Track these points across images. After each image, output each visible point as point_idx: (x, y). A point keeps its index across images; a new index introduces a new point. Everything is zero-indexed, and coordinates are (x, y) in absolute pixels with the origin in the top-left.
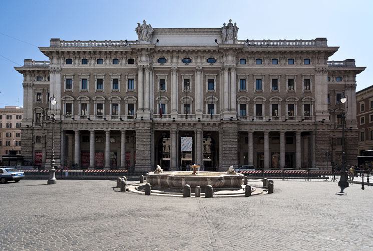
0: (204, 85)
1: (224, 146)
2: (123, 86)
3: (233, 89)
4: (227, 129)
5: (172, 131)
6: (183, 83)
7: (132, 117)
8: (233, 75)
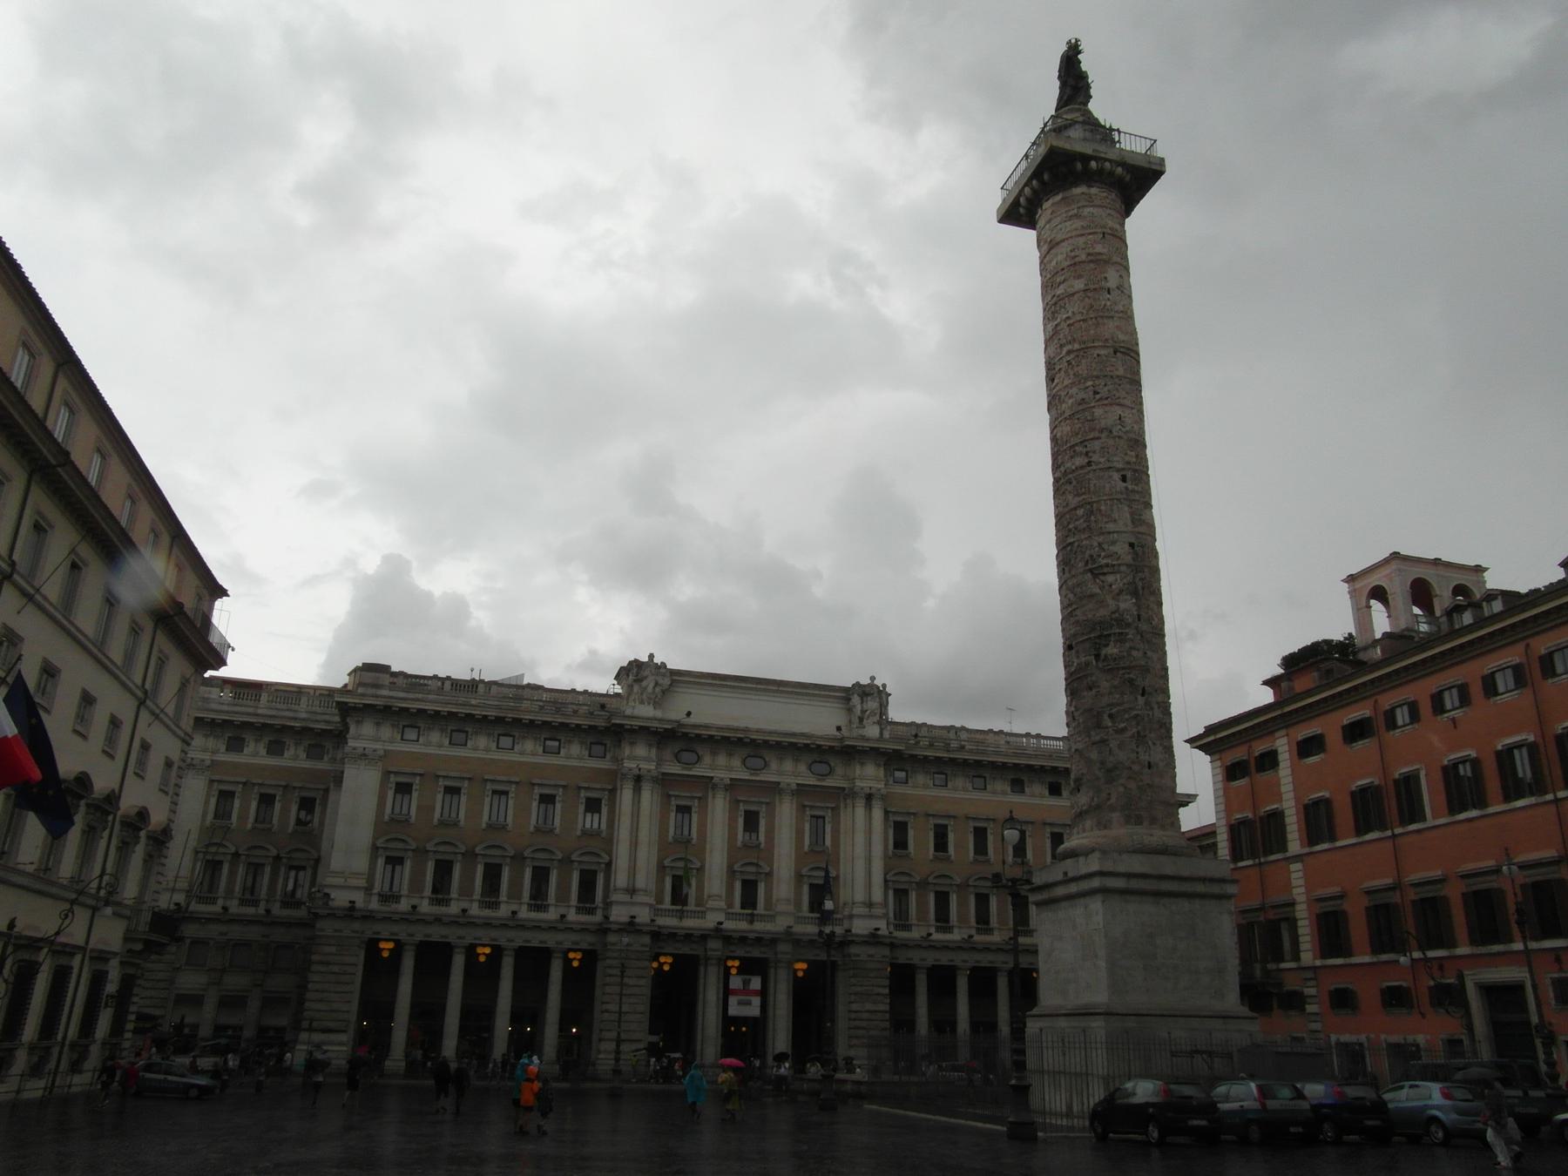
0: (799, 833)
1: (854, 1007)
3: (878, 849)
5: (707, 959)
6: (741, 821)
7: (591, 911)
8: (878, 814)
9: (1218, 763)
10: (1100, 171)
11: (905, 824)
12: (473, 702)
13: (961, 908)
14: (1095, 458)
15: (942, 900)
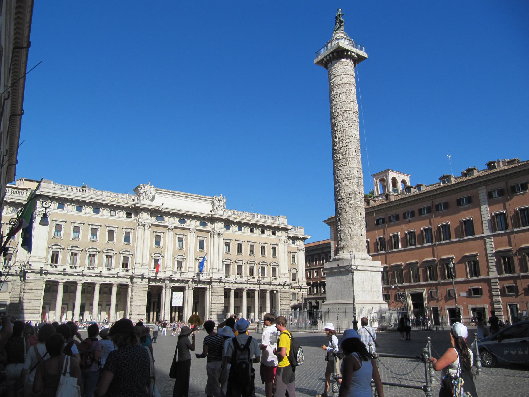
0: (196, 245)
2: (119, 237)
4: (216, 286)
7: (127, 271)
8: (221, 239)
9: (333, 228)
10: (351, 55)
11: (253, 245)
12: (84, 196)
13: (245, 270)
14: (349, 144)
15: (240, 267)
